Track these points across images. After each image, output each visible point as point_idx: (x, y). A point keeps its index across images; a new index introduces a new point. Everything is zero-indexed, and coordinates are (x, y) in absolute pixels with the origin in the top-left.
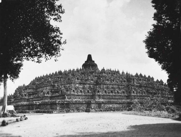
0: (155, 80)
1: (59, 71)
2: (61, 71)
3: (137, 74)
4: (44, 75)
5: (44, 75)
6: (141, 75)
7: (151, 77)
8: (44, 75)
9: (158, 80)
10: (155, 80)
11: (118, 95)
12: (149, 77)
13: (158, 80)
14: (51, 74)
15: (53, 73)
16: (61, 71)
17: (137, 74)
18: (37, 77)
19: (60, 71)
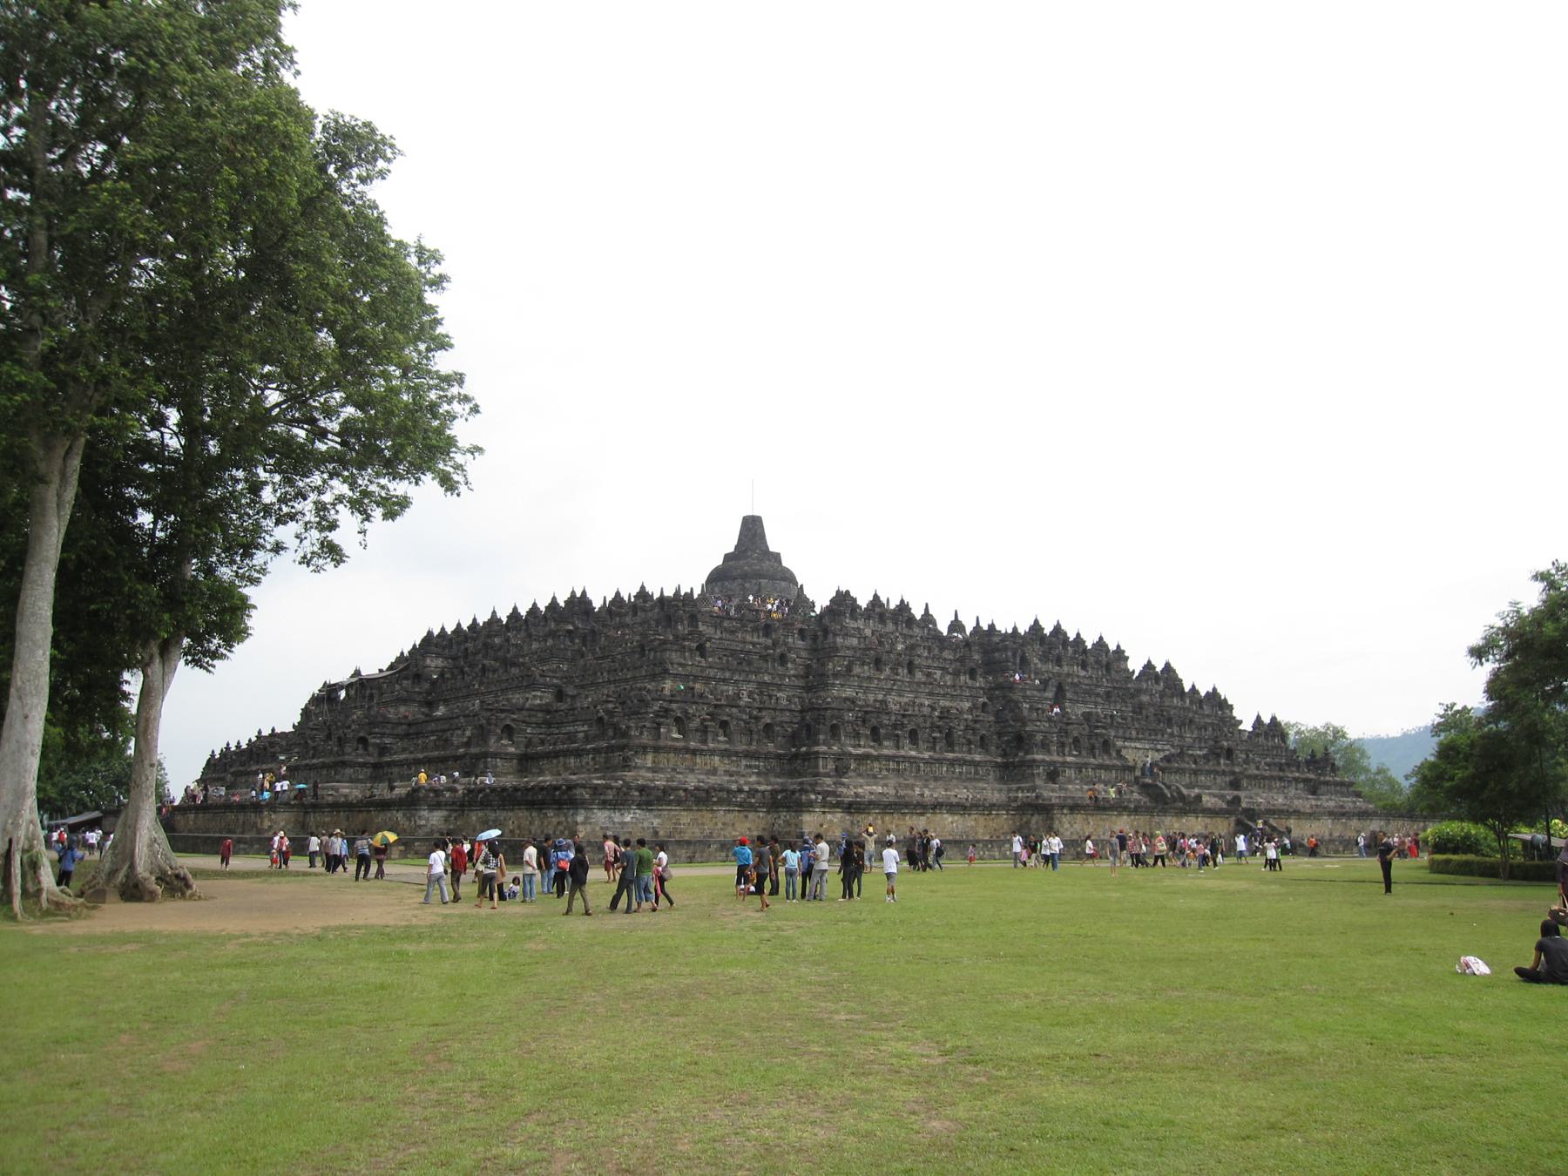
0: (1135, 665)
1: (573, 593)
2: (584, 593)
3: (1036, 627)
4: (475, 620)
5: (475, 620)
6: (1058, 629)
7: (1112, 647)
8: (480, 622)
9: (1149, 666)
10: (1135, 665)
11: (950, 755)
12: (1101, 644)
13: (1149, 666)
14: (523, 612)
15: (534, 609)
16: (584, 593)
17: (1036, 627)
18: (436, 632)
19: (578, 595)
